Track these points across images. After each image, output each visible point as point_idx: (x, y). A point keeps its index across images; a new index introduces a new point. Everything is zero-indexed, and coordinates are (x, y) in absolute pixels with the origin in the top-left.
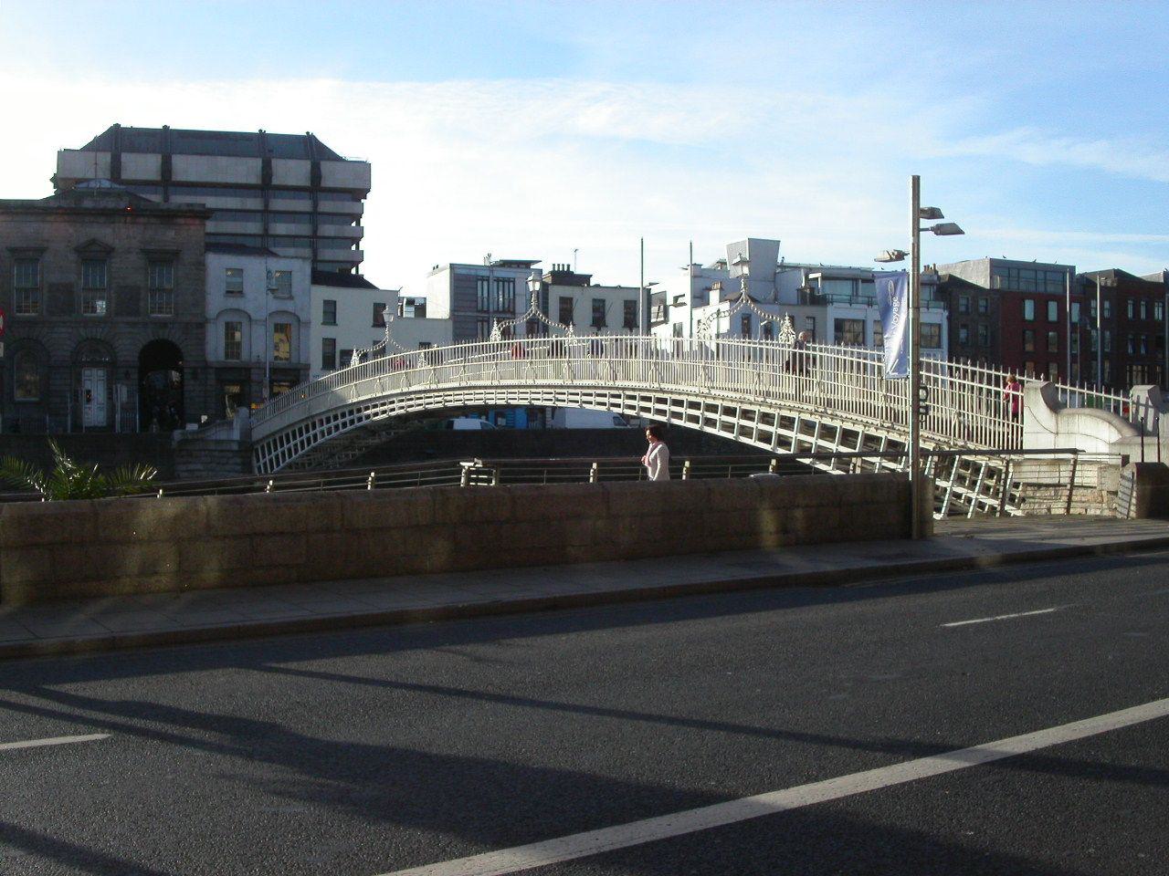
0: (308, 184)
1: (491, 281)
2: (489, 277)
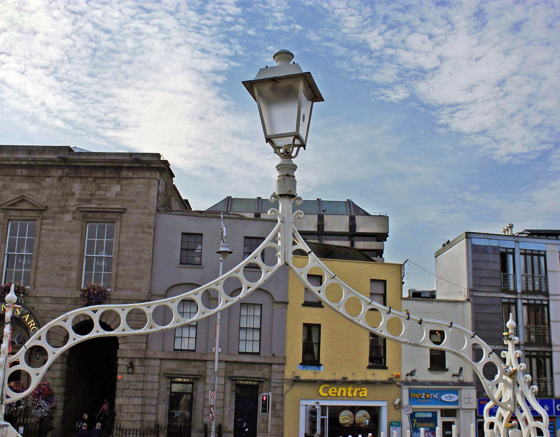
0: (347, 230)
1: (517, 254)
2: (514, 249)
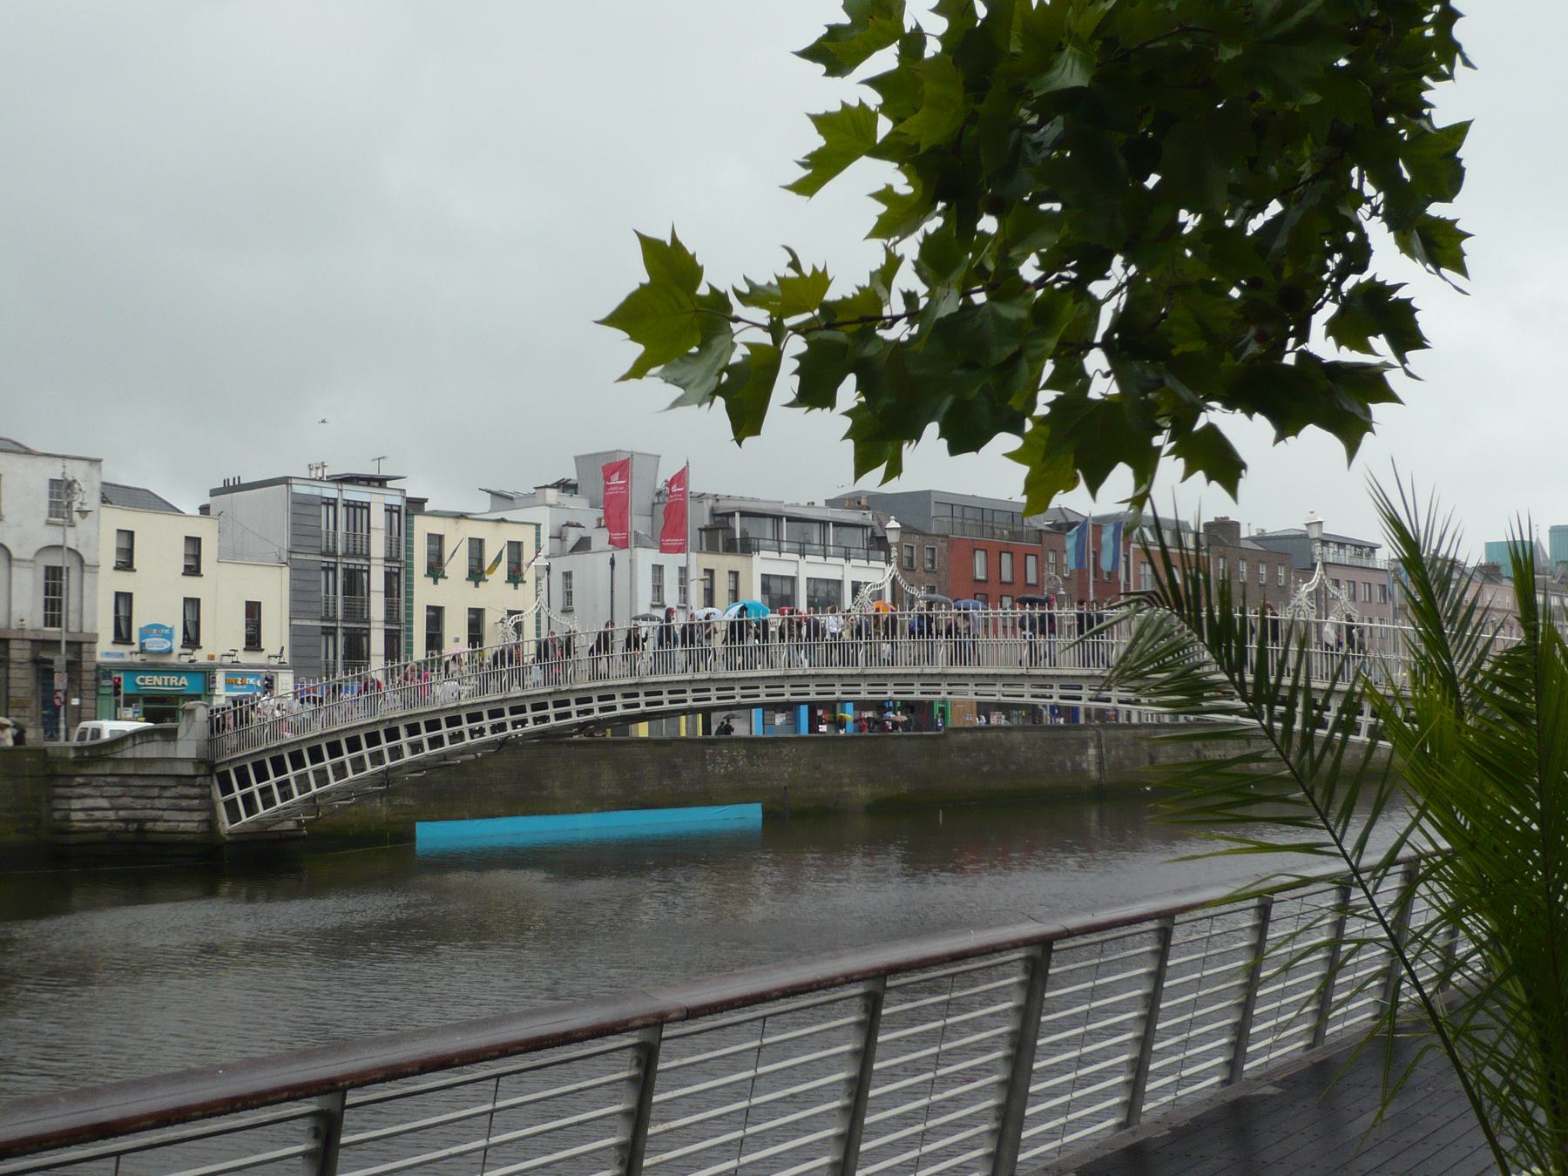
1: (340, 506)
